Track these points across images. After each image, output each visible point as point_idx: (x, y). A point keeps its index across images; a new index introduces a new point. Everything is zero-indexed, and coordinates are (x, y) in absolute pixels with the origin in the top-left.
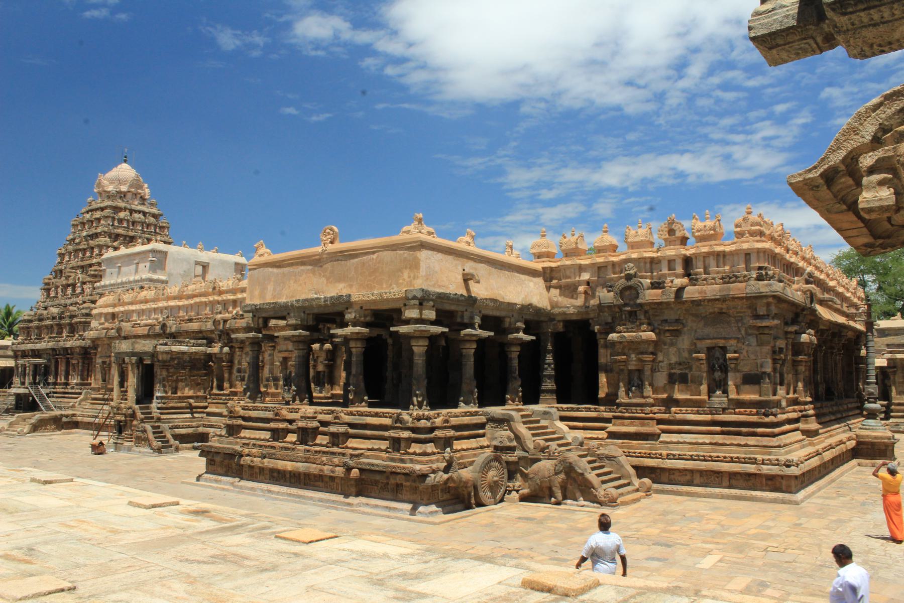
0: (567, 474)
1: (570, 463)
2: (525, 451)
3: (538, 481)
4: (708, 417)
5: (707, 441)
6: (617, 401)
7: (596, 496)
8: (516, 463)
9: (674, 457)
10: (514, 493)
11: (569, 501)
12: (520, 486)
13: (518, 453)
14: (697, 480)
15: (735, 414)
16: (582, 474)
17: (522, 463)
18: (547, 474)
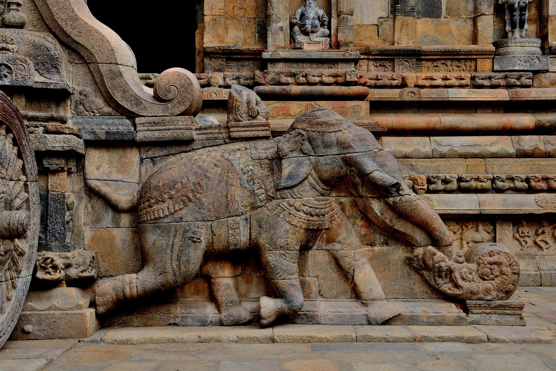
1: (343, 145)
4: (502, 95)
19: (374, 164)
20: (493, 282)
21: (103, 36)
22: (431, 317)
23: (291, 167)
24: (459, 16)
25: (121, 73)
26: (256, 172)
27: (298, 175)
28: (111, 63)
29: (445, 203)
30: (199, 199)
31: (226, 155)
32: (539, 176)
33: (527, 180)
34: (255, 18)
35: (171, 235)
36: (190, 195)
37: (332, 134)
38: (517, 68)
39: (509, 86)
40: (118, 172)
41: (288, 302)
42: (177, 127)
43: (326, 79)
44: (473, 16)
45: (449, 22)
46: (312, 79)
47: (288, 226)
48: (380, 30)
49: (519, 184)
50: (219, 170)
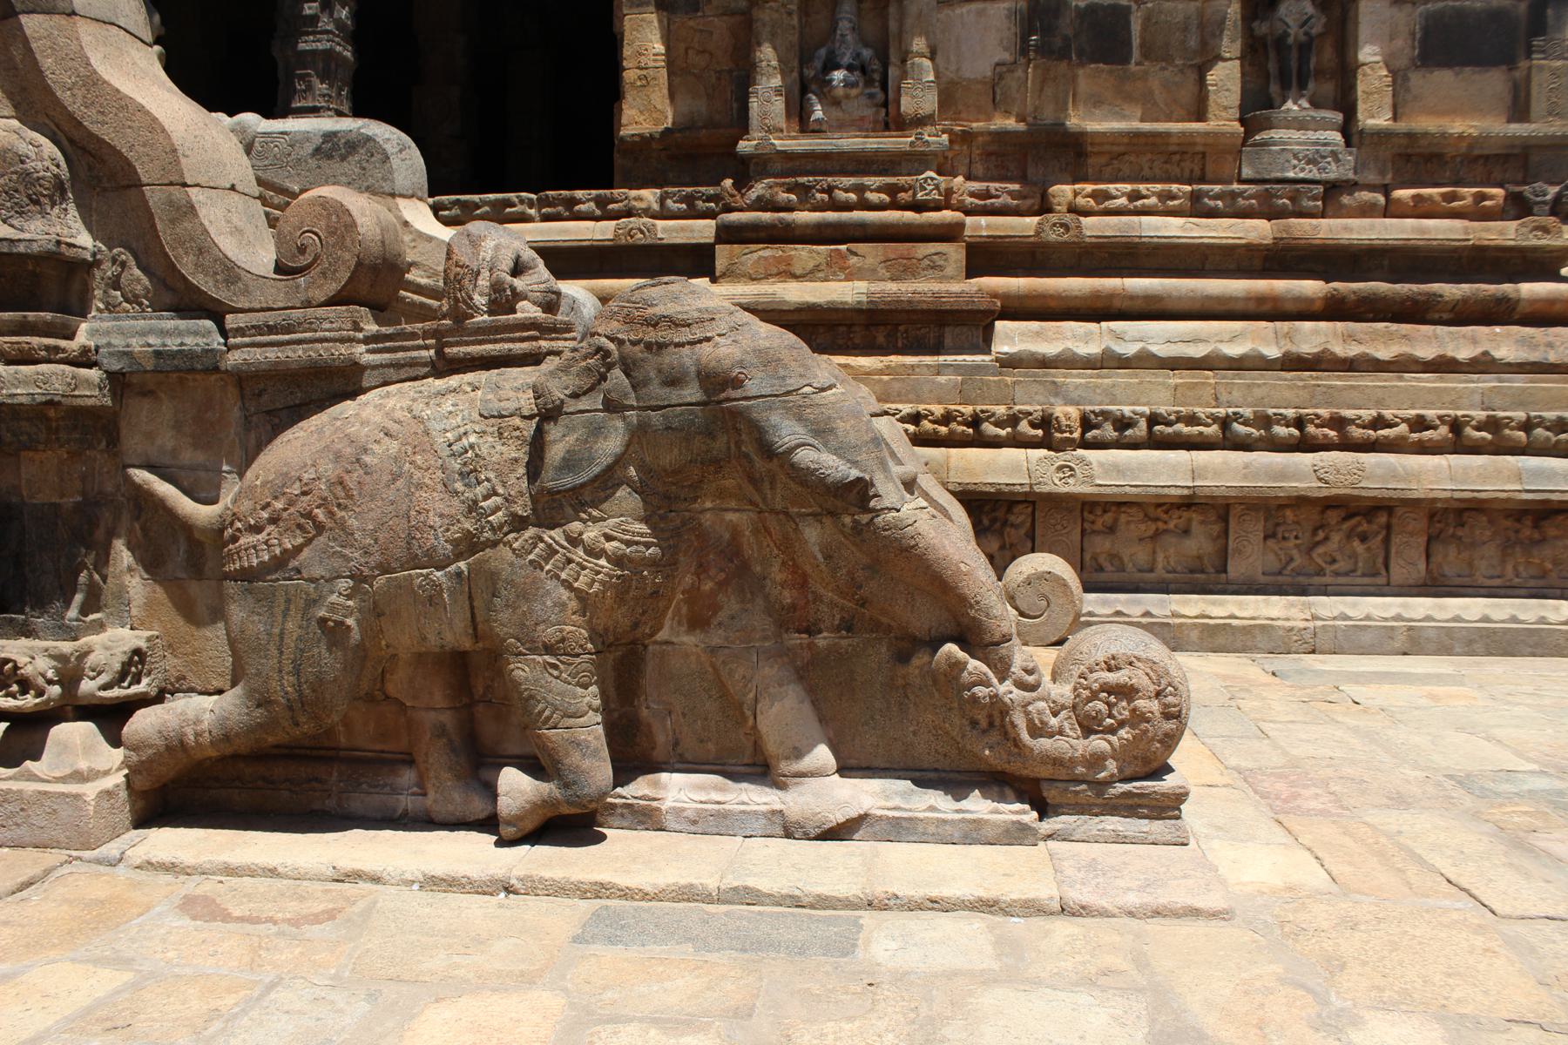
0: (665, 502)
2: (190, 304)
3: (338, 600)
4: (1257, 230)
5: (1273, 352)
6: (744, 146)
7: (996, 717)
8: (88, 429)
9: (1124, 433)
10: (74, 739)
11: (677, 790)
12: (135, 663)
13: (116, 330)
14: (1251, 556)
15: (1391, 210)
16: (859, 493)
17: (152, 426)
18: (440, 514)
19: (800, 429)
20: (1114, 739)
21: (155, 119)
22: (944, 821)
23: (571, 439)
24: (1168, 59)
25: (193, 207)
26: (484, 451)
27: (591, 460)
28: (171, 184)
29: (1118, 469)
30: (342, 525)
31: (418, 407)
32: (1324, 412)
33: (1299, 423)
34: (730, 71)
35: (278, 611)
36: (320, 514)
37: (686, 350)
38: (1291, 174)
39: (1271, 214)
40: (195, 446)
41: (566, 786)
42: (319, 334)
43: (873, 197)
44: (1197, 61)
45: (1146, 73)
46: (841, 195)
47: (565, 594)
48: (998, 91)
49: (1281, 431)
50: (394, 446)
